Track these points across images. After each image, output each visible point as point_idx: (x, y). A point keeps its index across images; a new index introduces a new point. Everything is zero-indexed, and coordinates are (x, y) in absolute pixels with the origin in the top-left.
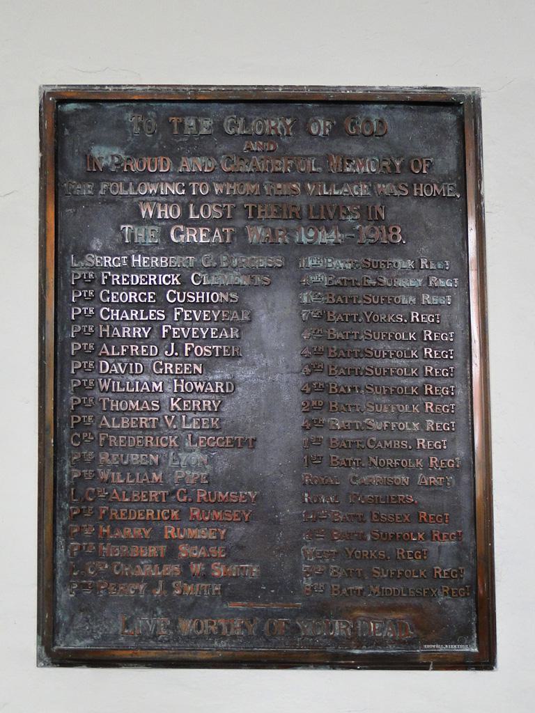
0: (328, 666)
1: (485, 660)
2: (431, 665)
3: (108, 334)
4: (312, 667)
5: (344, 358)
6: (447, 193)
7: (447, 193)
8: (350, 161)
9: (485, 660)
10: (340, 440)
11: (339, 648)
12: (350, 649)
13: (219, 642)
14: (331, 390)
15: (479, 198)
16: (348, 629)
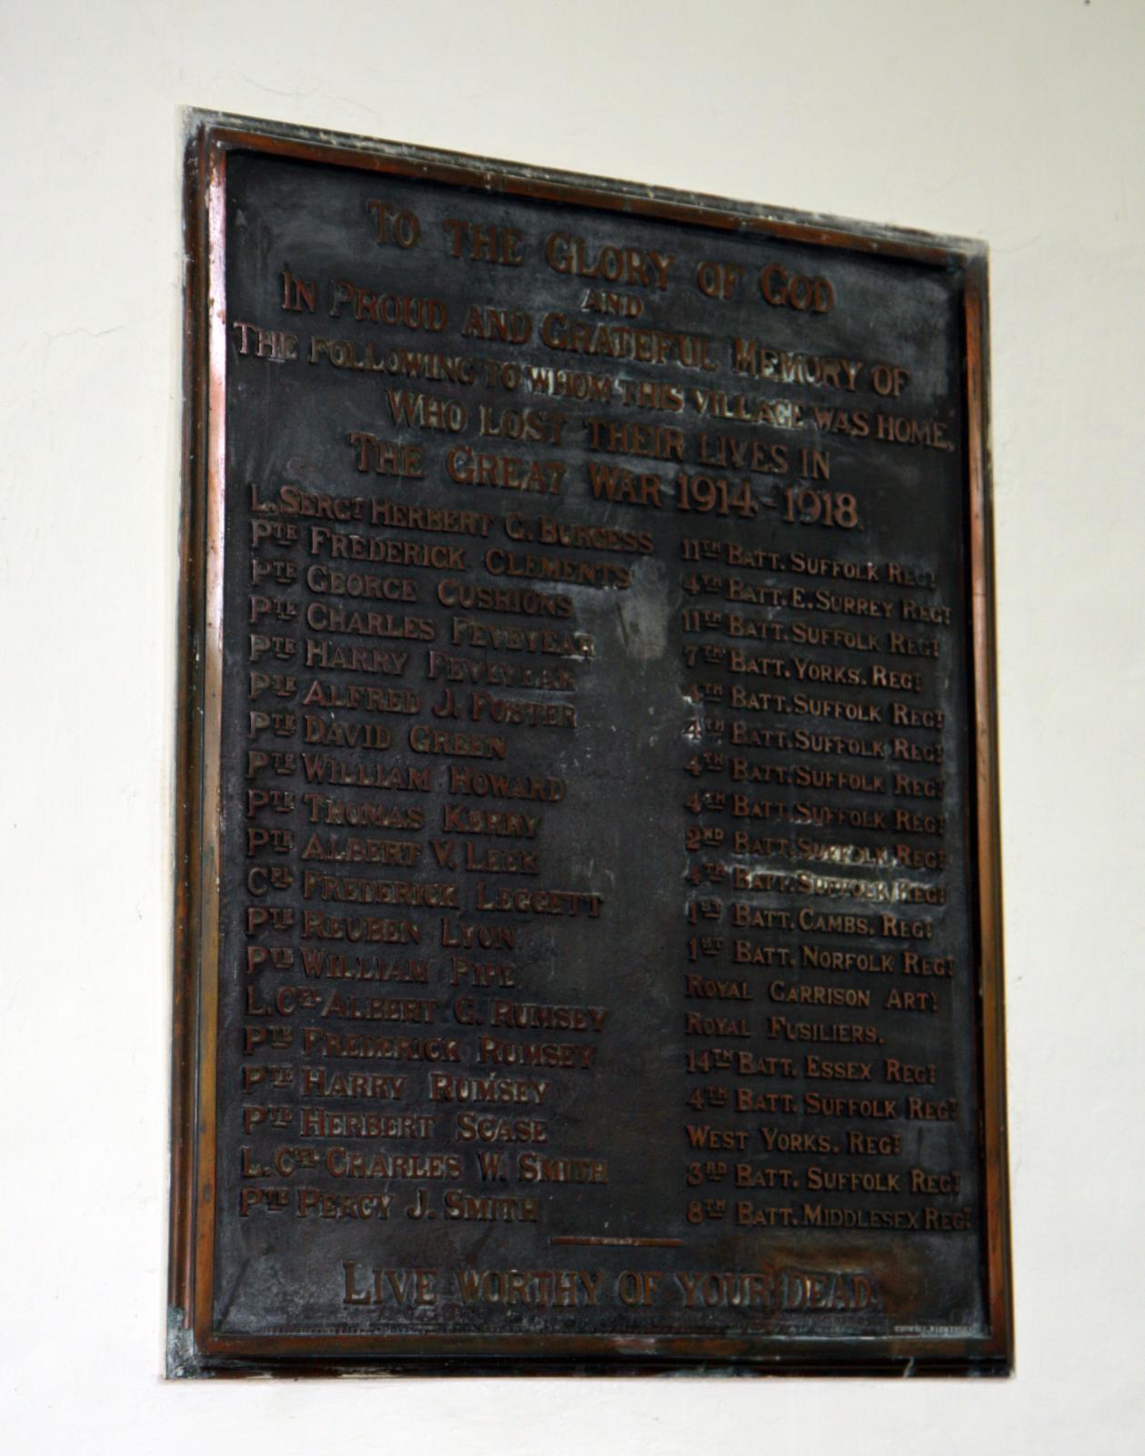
0: (731, 1369)
1: (991, 1358)
2: (910, 1364)
3: (324, 657)
4: (702, 1370)
5: (759, 746)
6: (932, 440)
7: (932, 440)
8: (769, 356)
9: (991, 1358)
10: (753, 910)
11: (750, 1331)
12: (769, 1333)
13: (531, 1320)
14: (737, 809)
15: (986, 456)
16: (766, 1293)
